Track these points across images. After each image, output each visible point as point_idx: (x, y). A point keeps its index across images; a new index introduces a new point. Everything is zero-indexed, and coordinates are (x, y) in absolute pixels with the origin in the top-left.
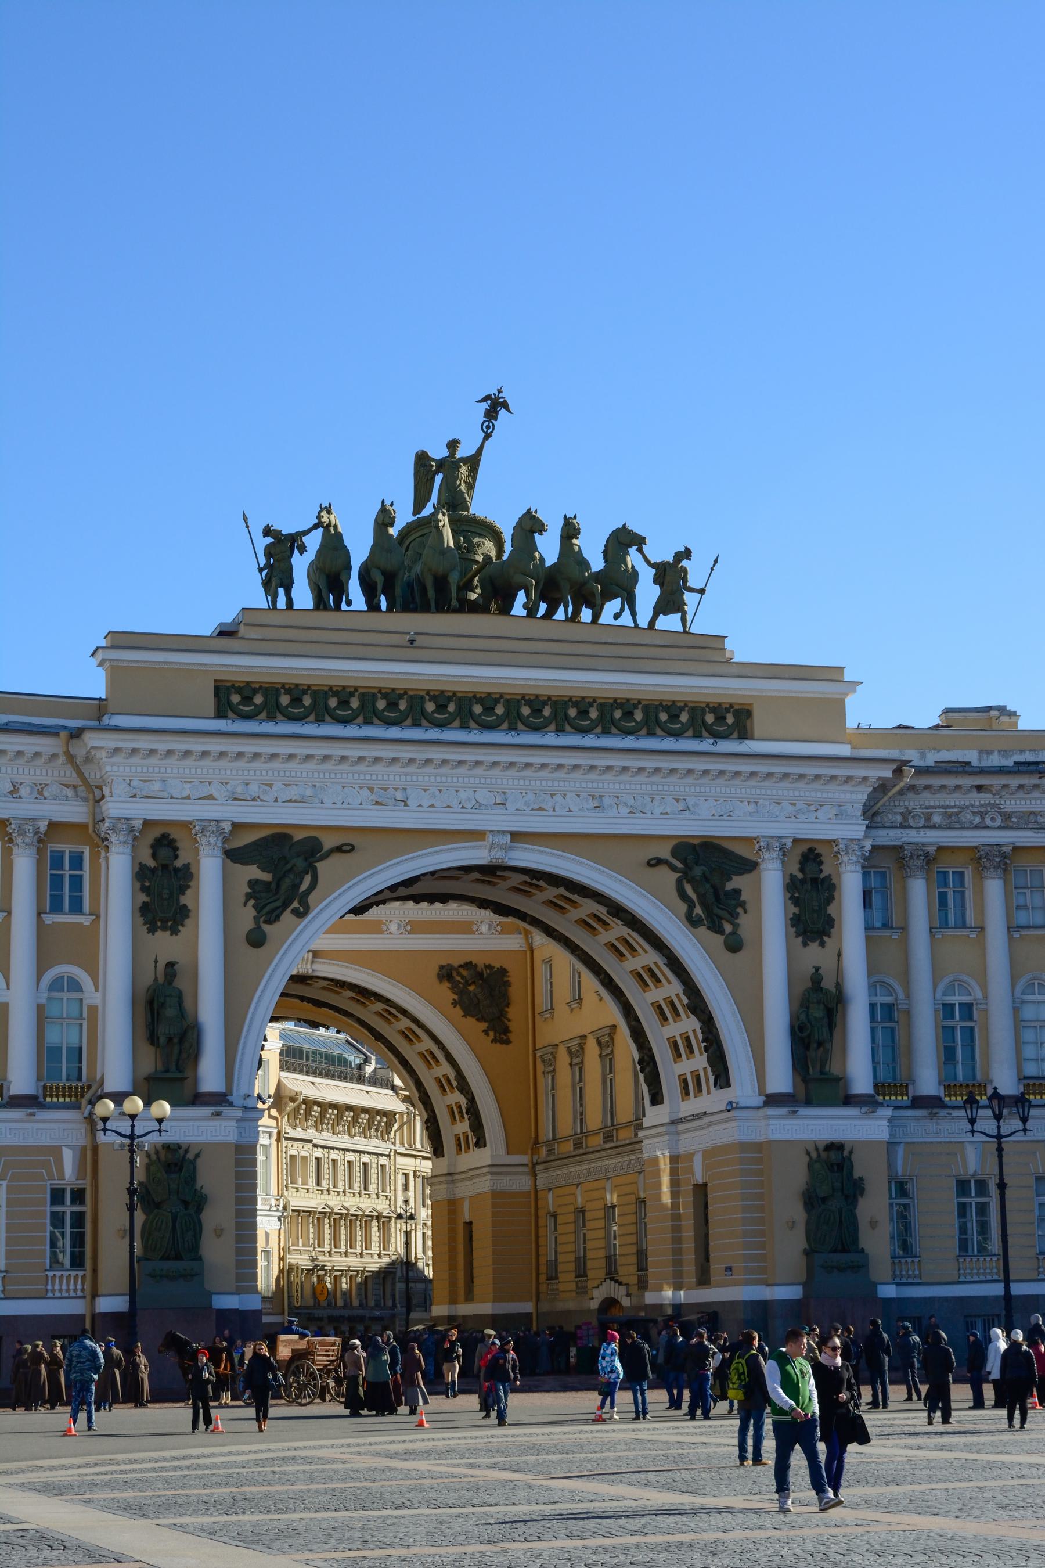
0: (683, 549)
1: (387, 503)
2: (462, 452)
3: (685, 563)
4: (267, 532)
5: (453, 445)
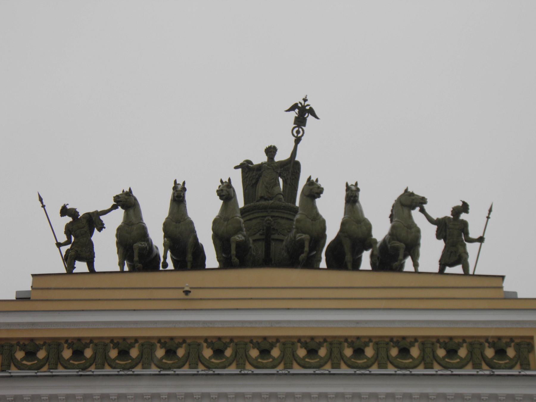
0: (460, 204)
1: (180, 182)
2: (280, 157)
3: (463, 216)
4: (65, 211)
5: (271, 151)
